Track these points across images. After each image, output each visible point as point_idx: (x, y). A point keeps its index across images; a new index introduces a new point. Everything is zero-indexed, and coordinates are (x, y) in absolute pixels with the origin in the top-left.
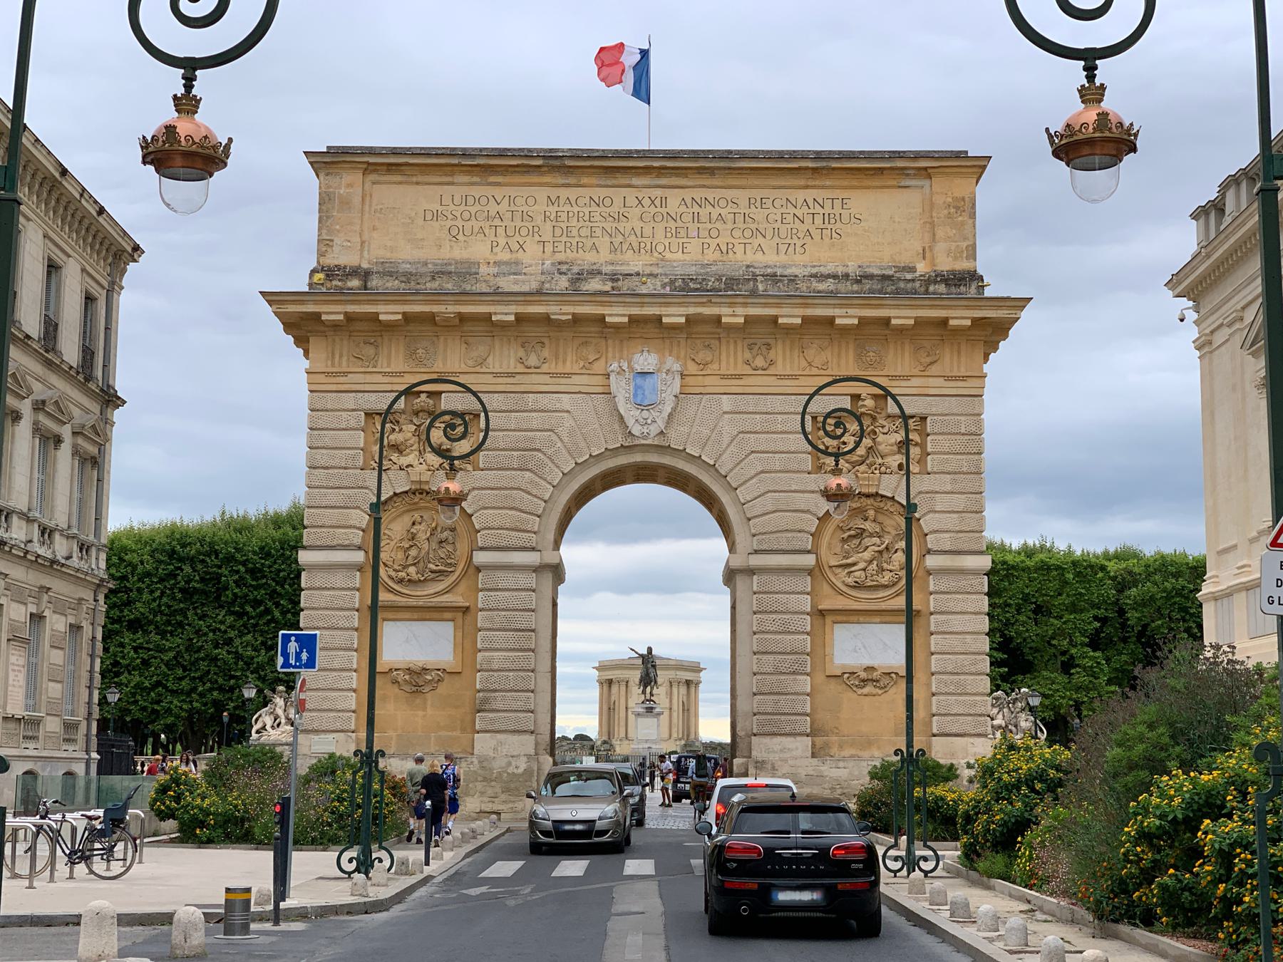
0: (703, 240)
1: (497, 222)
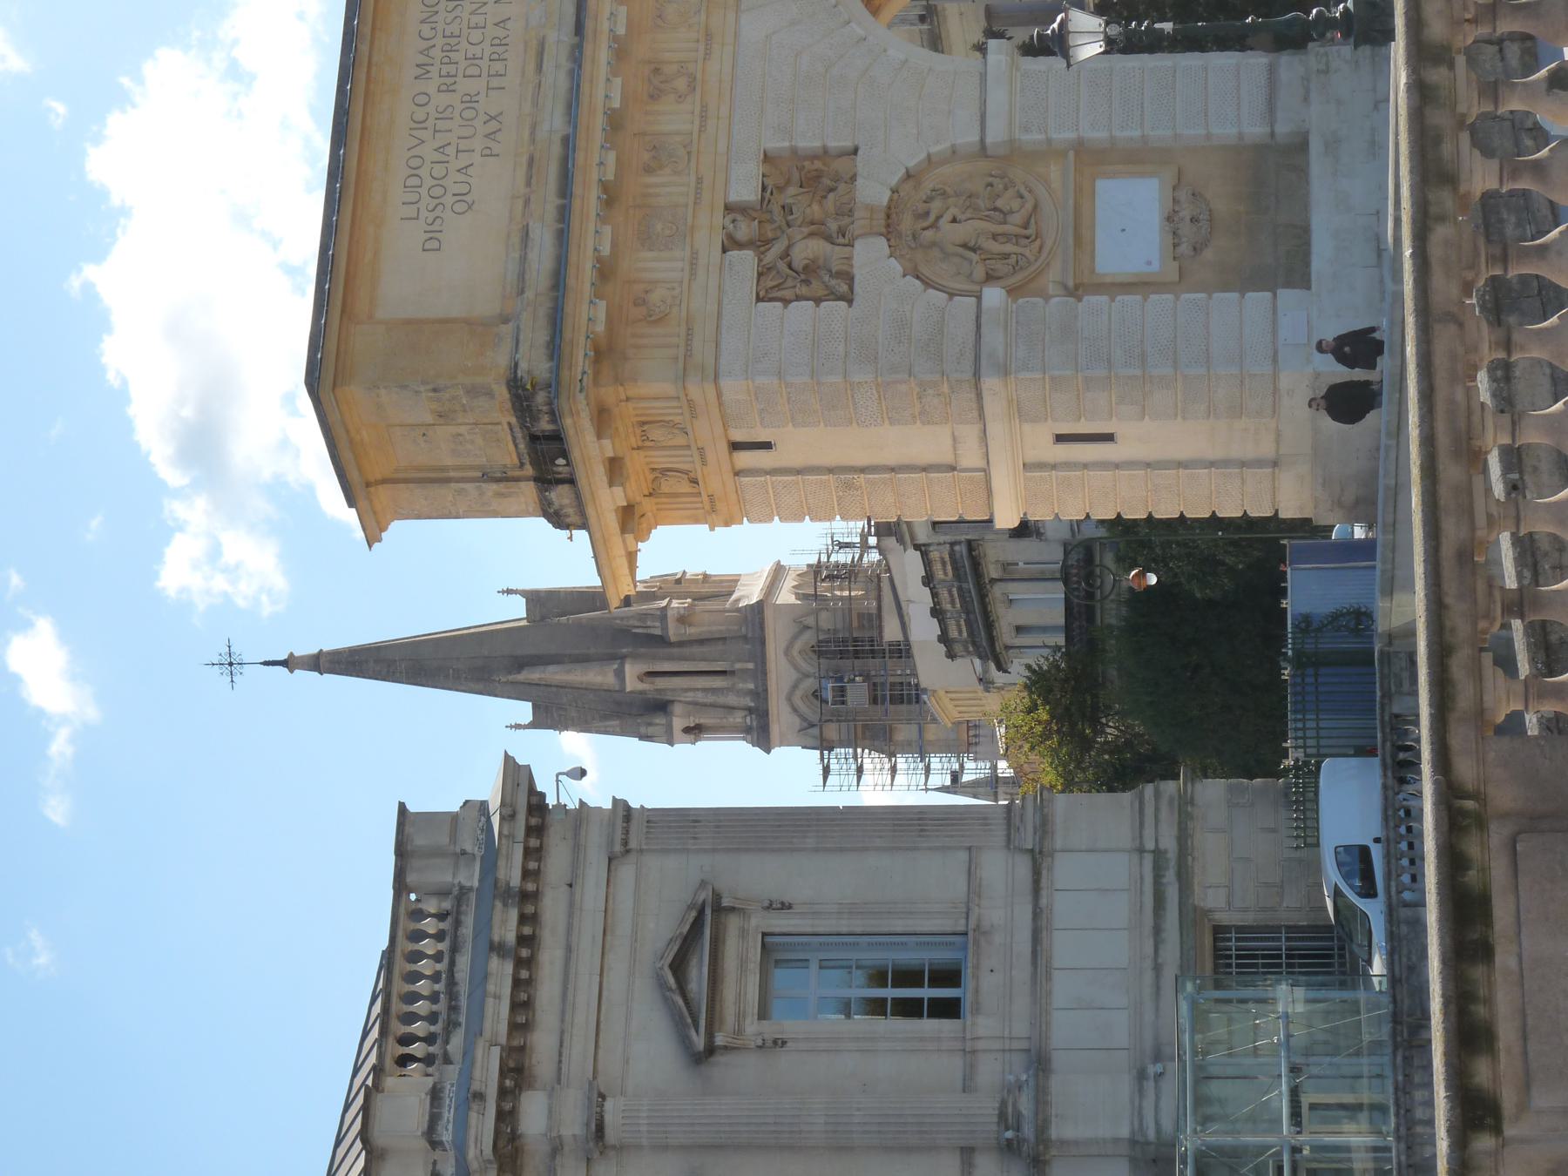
1: (451, 150)
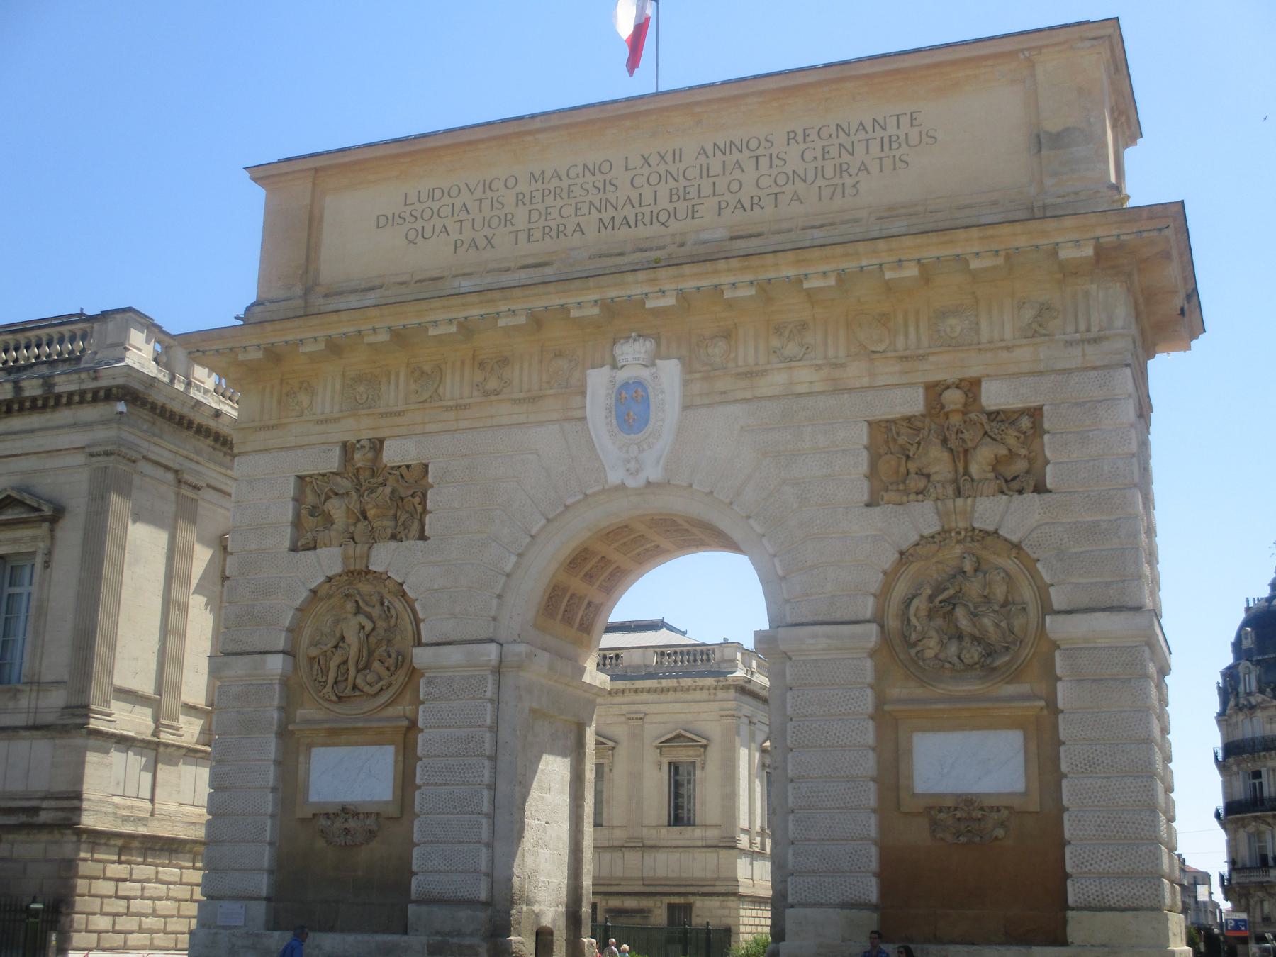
0: (720, 198)
1: (463, 216)
